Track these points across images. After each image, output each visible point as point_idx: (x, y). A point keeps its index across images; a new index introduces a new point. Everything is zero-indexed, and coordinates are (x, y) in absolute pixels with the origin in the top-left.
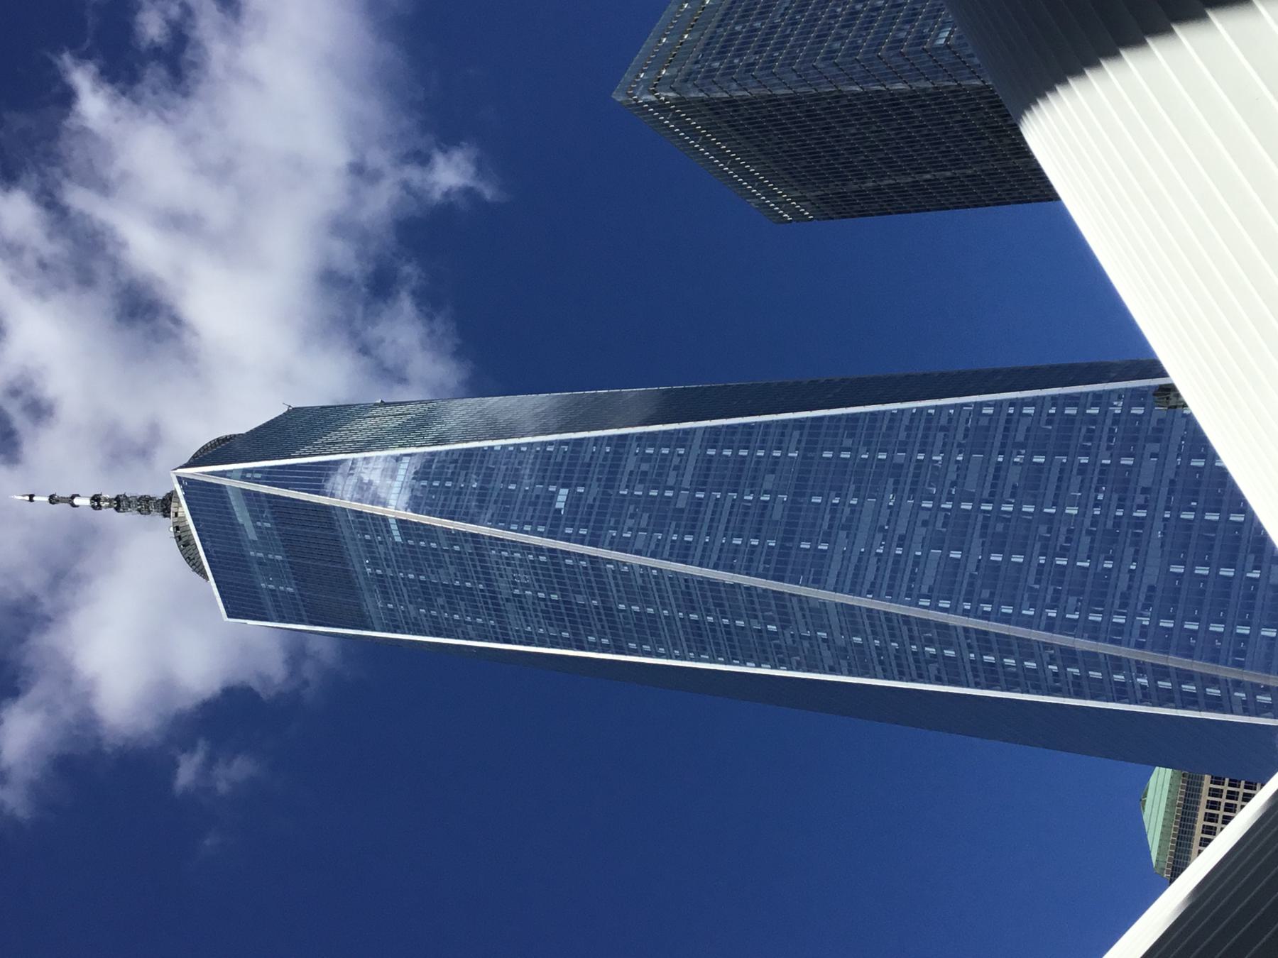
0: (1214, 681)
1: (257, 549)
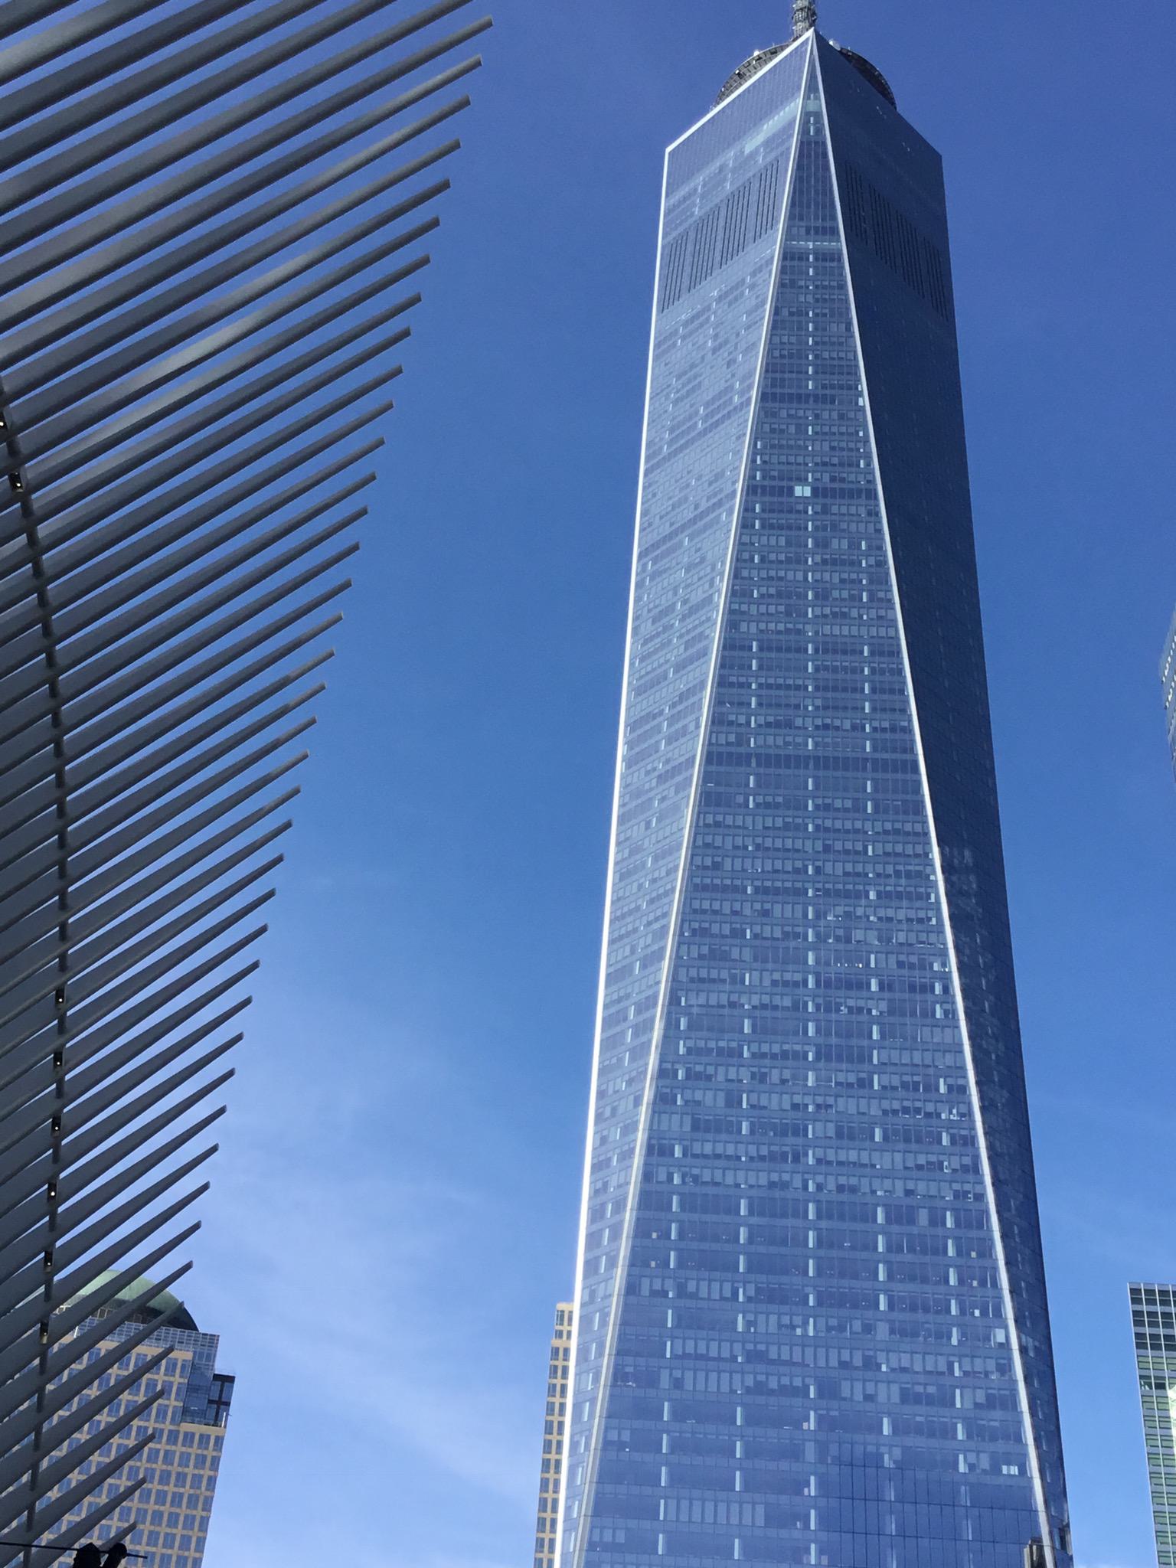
0: (612, 1263)
1: (736, 157)
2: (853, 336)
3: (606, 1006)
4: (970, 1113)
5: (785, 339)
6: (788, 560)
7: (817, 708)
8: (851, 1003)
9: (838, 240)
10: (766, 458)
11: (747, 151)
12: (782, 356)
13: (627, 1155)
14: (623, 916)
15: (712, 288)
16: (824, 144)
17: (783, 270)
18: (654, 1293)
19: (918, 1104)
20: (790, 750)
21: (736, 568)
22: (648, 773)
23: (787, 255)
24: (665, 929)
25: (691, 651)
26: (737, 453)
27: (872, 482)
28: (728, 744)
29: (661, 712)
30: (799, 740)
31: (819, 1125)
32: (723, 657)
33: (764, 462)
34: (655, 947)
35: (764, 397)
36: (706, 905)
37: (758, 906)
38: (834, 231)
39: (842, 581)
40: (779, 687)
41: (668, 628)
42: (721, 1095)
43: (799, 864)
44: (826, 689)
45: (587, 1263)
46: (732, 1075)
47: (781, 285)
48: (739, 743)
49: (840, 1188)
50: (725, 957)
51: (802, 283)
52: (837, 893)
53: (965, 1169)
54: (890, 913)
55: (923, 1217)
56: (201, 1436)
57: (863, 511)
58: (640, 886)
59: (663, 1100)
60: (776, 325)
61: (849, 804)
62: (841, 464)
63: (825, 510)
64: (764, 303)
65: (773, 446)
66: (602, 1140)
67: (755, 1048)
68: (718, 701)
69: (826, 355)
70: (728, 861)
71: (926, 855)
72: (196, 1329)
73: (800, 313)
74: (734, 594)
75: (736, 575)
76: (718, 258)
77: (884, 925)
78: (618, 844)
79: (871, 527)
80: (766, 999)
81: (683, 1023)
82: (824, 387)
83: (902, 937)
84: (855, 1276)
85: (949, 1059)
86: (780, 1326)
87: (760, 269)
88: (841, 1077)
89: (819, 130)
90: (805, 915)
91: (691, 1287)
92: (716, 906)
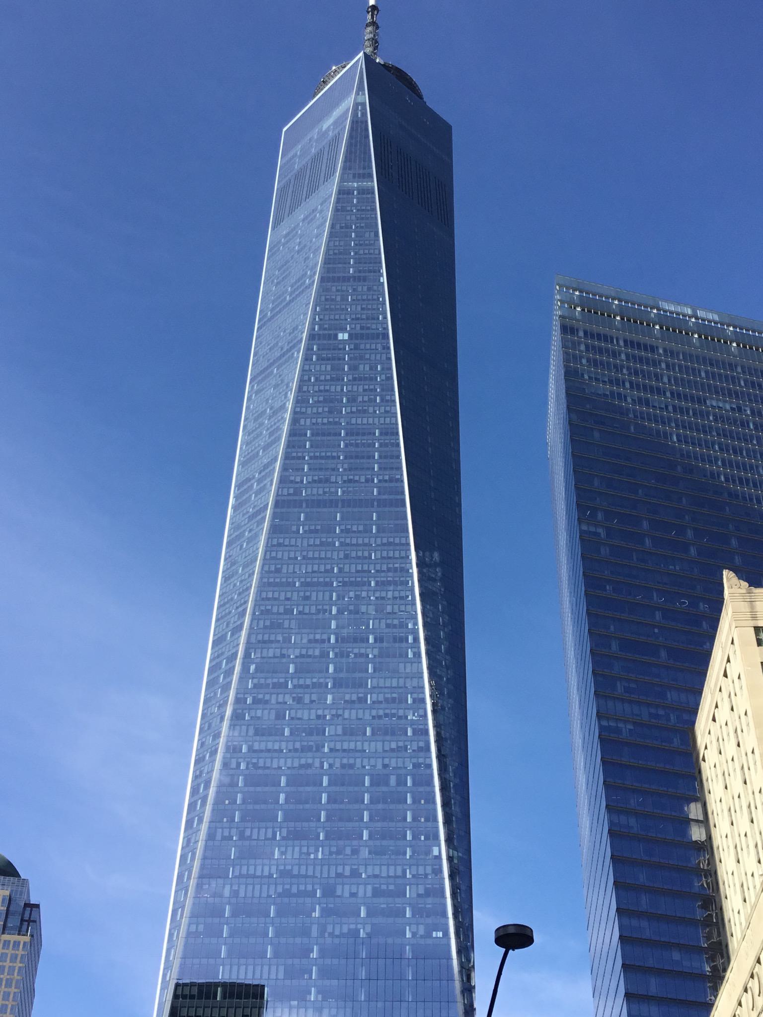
2: (379, 240)
3: (211, 661)
4: (425, 715)
5: (337, 243)
6: (332, 379)
7: (345, 470)
8: (356, 651)
9: (373, 181)
10: (322, 317)
11: (324, 128)
12: (335, 254)
13: (214, 753)
14: (224, 604)
15: (300, 214)
16: (367, 122)
17: (338, 200)
18: (224, 838)
19: (394, 711)
20: (326, 497)
21: (300, 386)
22: (244, 515)
23: (340, 192)
24: (245, 610)
25: (273, 438)
26: (306, 314)
27: (386, 329)
28: (289, 495)
29: (254, 477)
30: (333, 490)
31: (333, 727)
32: (289, 441)
33: (321, 320)
34: (239, 623)
35: (322, 279)
36: (270, 595)
37: (302, 594)
38: (371, 176)
39: (365, 390)
40: (321, 458)
41: (261, 424)
42: (273, 712)
43: (328, 567)
44: (351, 457)
45: (187, 822)
46: (281, 699)
47: (336, 210)
48: (295, 494)
49: (343, 766)
50: (280, 626)
51: (349, 208)
52: (352, 584)
53: (420, 749)
54: (383, 594)
55: (393, 780)
56: (15, 942)
57: (379, 347)
58: (235, 585)
59: (237, 717)
60: (331, 235)
61: (361, 528)
62: (368, 319)
63: (356, 347)
64: (326, 221)
65: (326, 310)
66: (202, 744)
67: (295, 681)
68: (284, 468)
69: (361, 252)
70: (285, 567)
71: (408, 557)
72: (19, 876)
73: (347, 227)
74: (297, 401)
75: (300, 389)
76: (304, 197)
77: (380, 602)
78: (226, 559)
79: (384, 357)
80: (304, 652)
81: (253, 667)
82: (360, 272)
83: (389, 609)
84: (350, 820)
85: (415, 682)
86: (301, 853)
87: (325, 201)
88: (347, 697)
89: (364, 114)
90: (331, 598)
91: (248, 833)
92: (276, 595)
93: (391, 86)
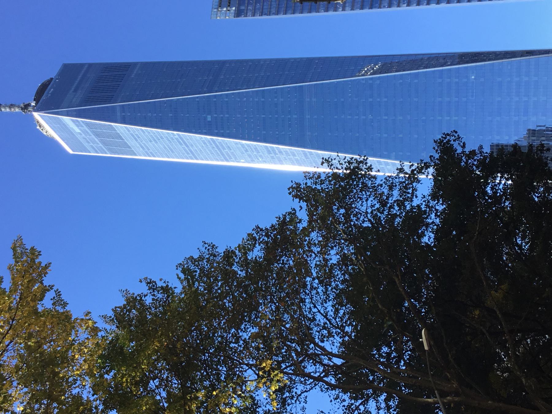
11: (79, 131)
15: (131, 142)
93: (50, 97)
